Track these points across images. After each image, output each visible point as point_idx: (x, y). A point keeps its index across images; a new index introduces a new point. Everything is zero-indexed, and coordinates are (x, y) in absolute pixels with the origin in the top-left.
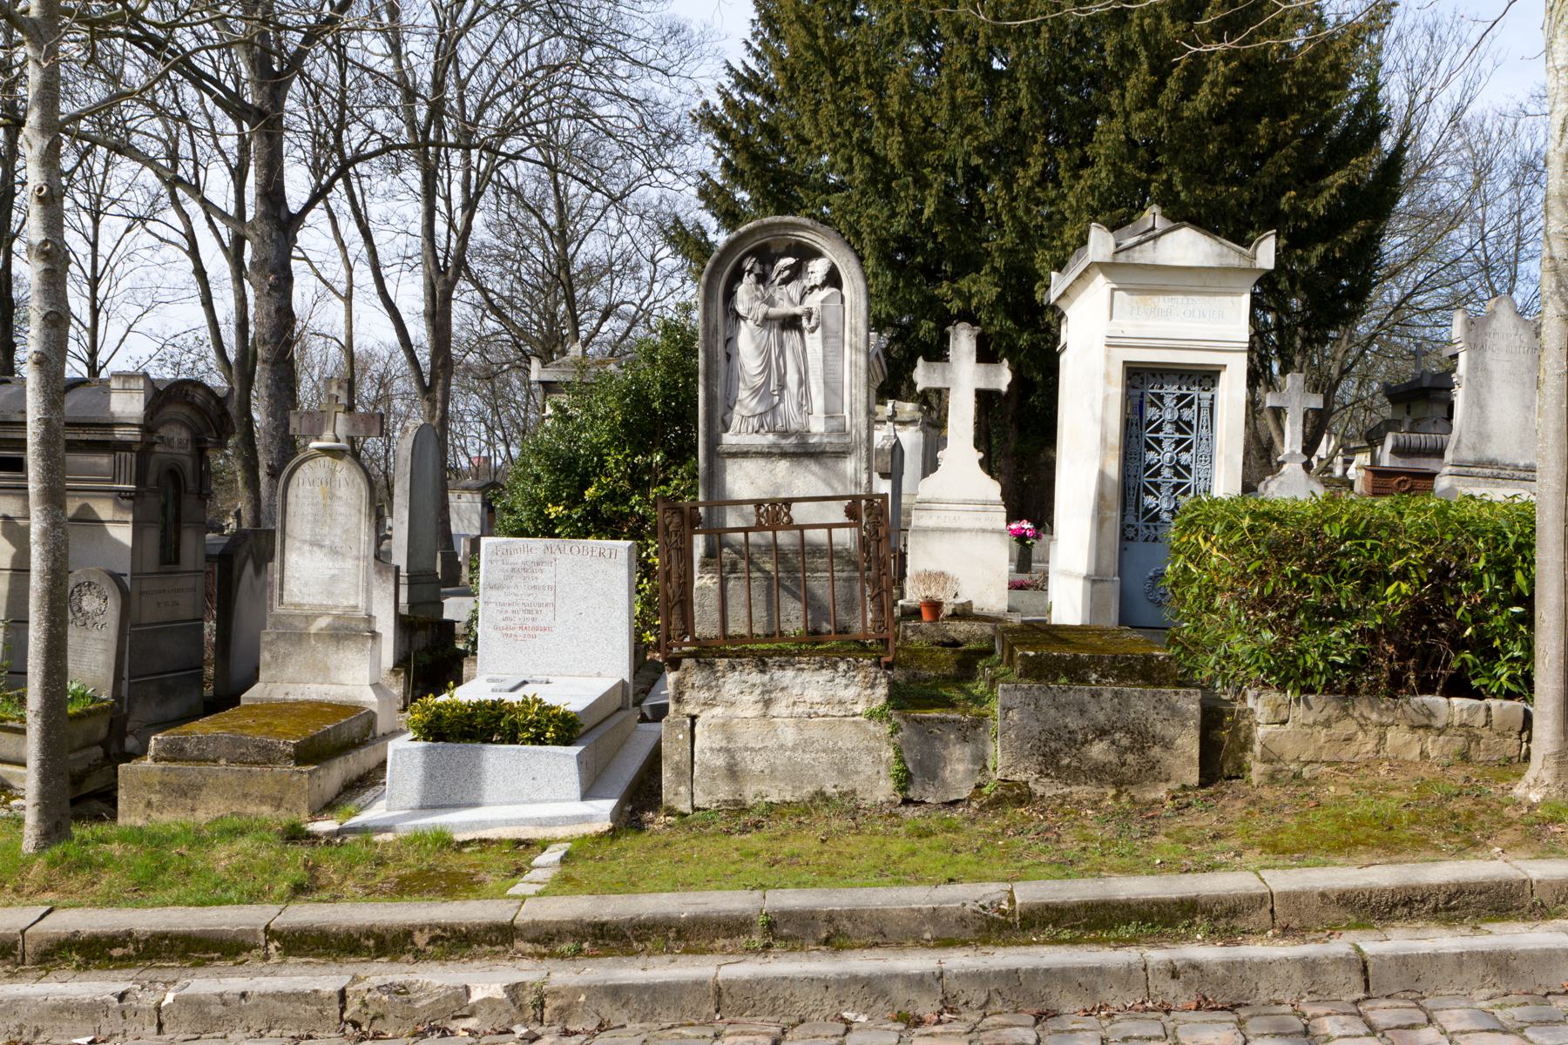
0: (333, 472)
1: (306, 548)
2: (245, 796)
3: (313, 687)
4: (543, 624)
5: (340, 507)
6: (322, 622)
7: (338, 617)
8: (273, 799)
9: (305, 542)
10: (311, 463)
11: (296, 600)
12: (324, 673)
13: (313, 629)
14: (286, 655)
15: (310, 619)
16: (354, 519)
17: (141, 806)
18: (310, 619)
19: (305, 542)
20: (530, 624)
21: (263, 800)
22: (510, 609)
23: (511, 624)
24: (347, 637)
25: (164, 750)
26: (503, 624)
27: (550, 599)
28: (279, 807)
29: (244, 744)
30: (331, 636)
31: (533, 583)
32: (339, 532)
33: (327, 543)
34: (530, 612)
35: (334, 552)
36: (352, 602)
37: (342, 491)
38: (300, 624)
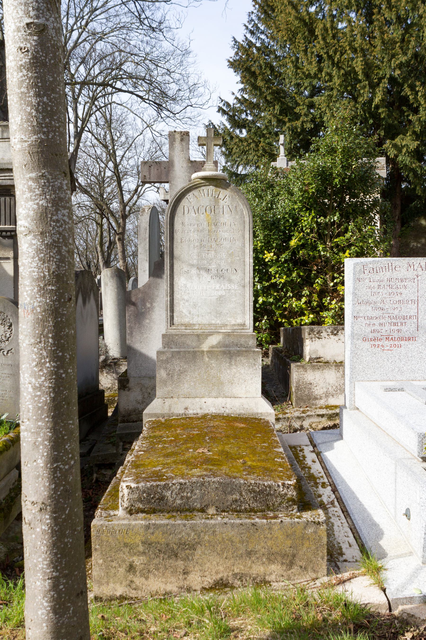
0: (217, 200)
1: (194, 271)
2: (249, 554)
3: (210, 401)
4: (407, 335)
5: (224, 233)
6: (214, 340)
7: (228, 335)
8: (284, 556)
9: (192, 265)
10: (195, 192)
11: (186, 320)
12: (218, 388)
13: (205, 347)
14: (181, 373)
15: (201, 337)
16: (238, 244)
17: (122, 570)
18: (201, 337)
19: (192, 265)
20: (396, 335)
21: (271, 557)
22: (377, 322)
23: (378, 335)
24: (239, 353)
25: (140, 500)
26: (371, 336)
27: (413, 312)
28: (291, 565)
29: (238, 489)
30: (224, 353)
31: (398, 298)
32: (224, 255)
33: (213, 266)
34: (395, 324)
35: (220, 275)
36: (239, 321)
37: (226, 218)
38: (192, 343)
